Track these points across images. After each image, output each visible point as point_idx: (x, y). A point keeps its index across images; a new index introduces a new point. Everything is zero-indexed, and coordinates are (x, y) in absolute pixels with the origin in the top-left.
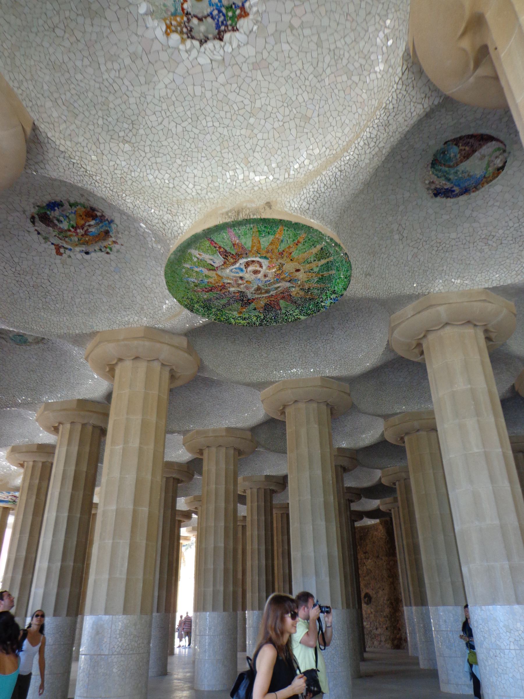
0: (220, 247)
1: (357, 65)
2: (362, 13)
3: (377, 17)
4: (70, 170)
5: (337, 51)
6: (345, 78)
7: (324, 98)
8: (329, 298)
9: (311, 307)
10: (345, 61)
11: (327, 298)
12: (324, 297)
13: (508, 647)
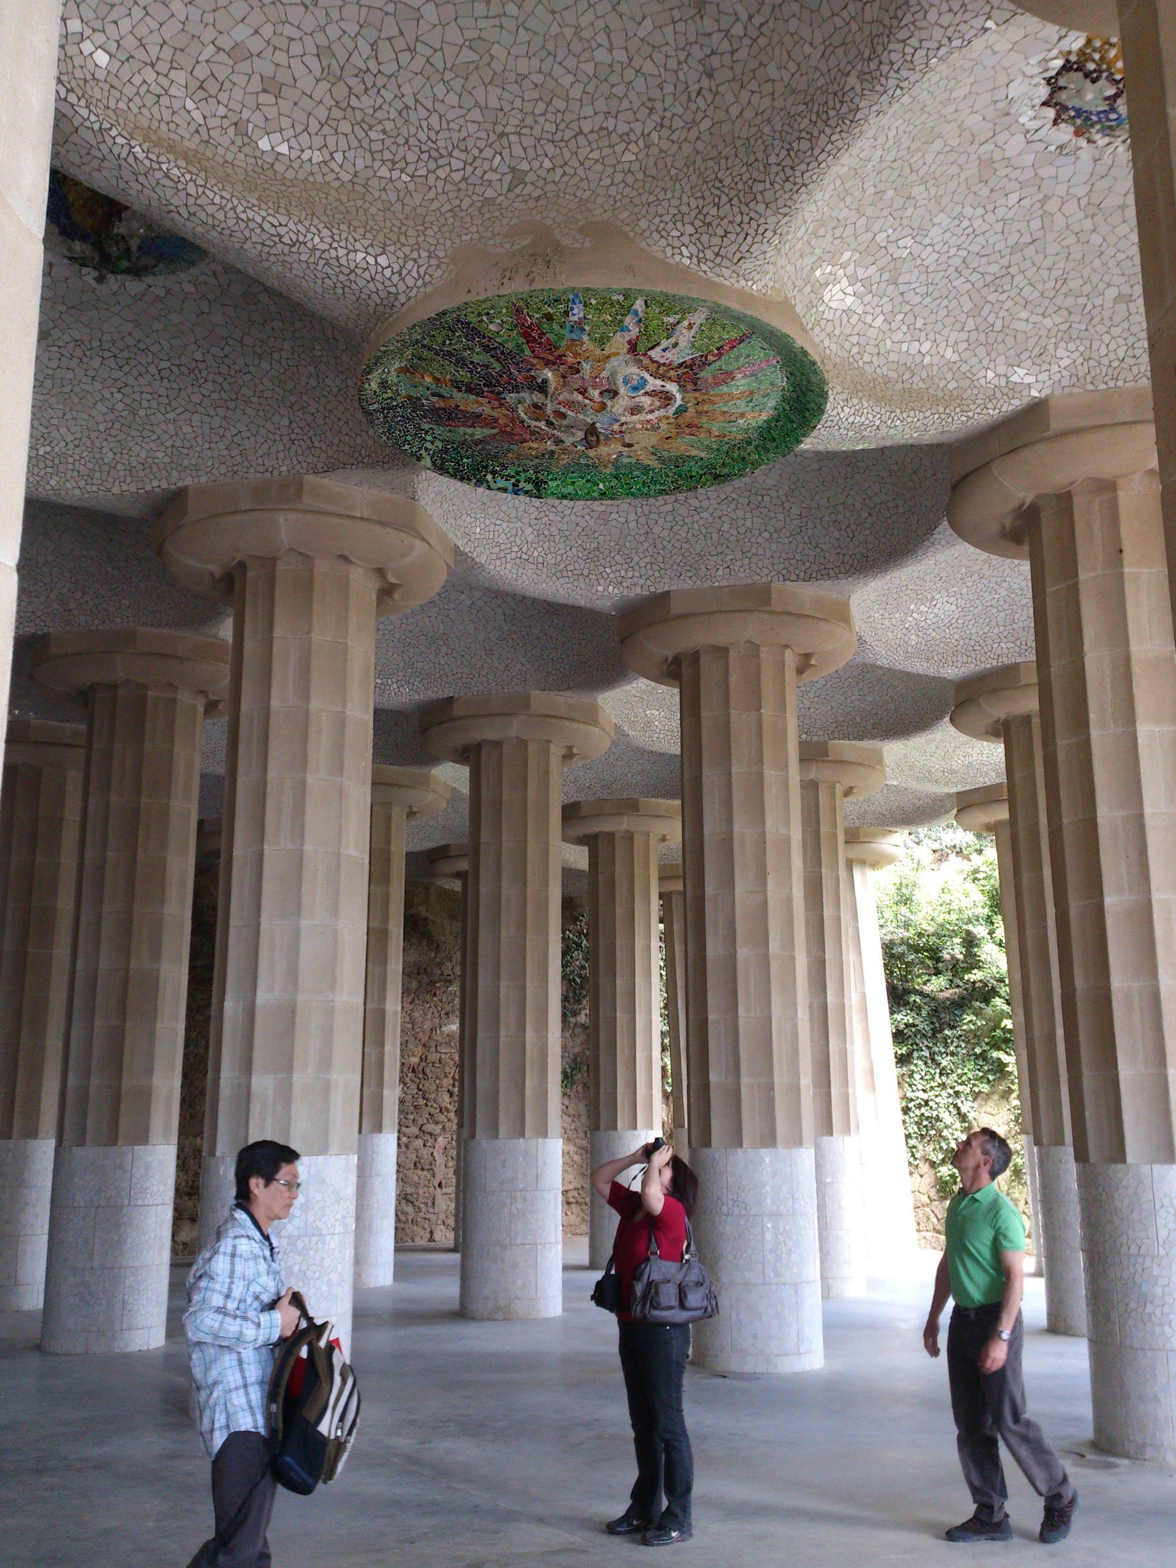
0: (720, 355)
1: (991, 319)
2: (1070, 301)
3: (1066, 326)
4: (945, 41)
5: (1008, 278)
6: (968, 306)
7: (931, 288)
8: (513, 480)
9: (465, 460)
10: (993, 297)
11: (513, 477)
12: (511, 471)
13: (331, 1231)
